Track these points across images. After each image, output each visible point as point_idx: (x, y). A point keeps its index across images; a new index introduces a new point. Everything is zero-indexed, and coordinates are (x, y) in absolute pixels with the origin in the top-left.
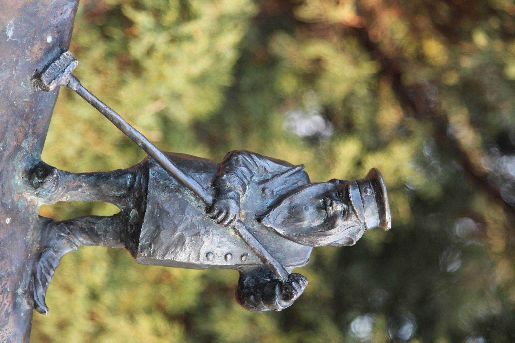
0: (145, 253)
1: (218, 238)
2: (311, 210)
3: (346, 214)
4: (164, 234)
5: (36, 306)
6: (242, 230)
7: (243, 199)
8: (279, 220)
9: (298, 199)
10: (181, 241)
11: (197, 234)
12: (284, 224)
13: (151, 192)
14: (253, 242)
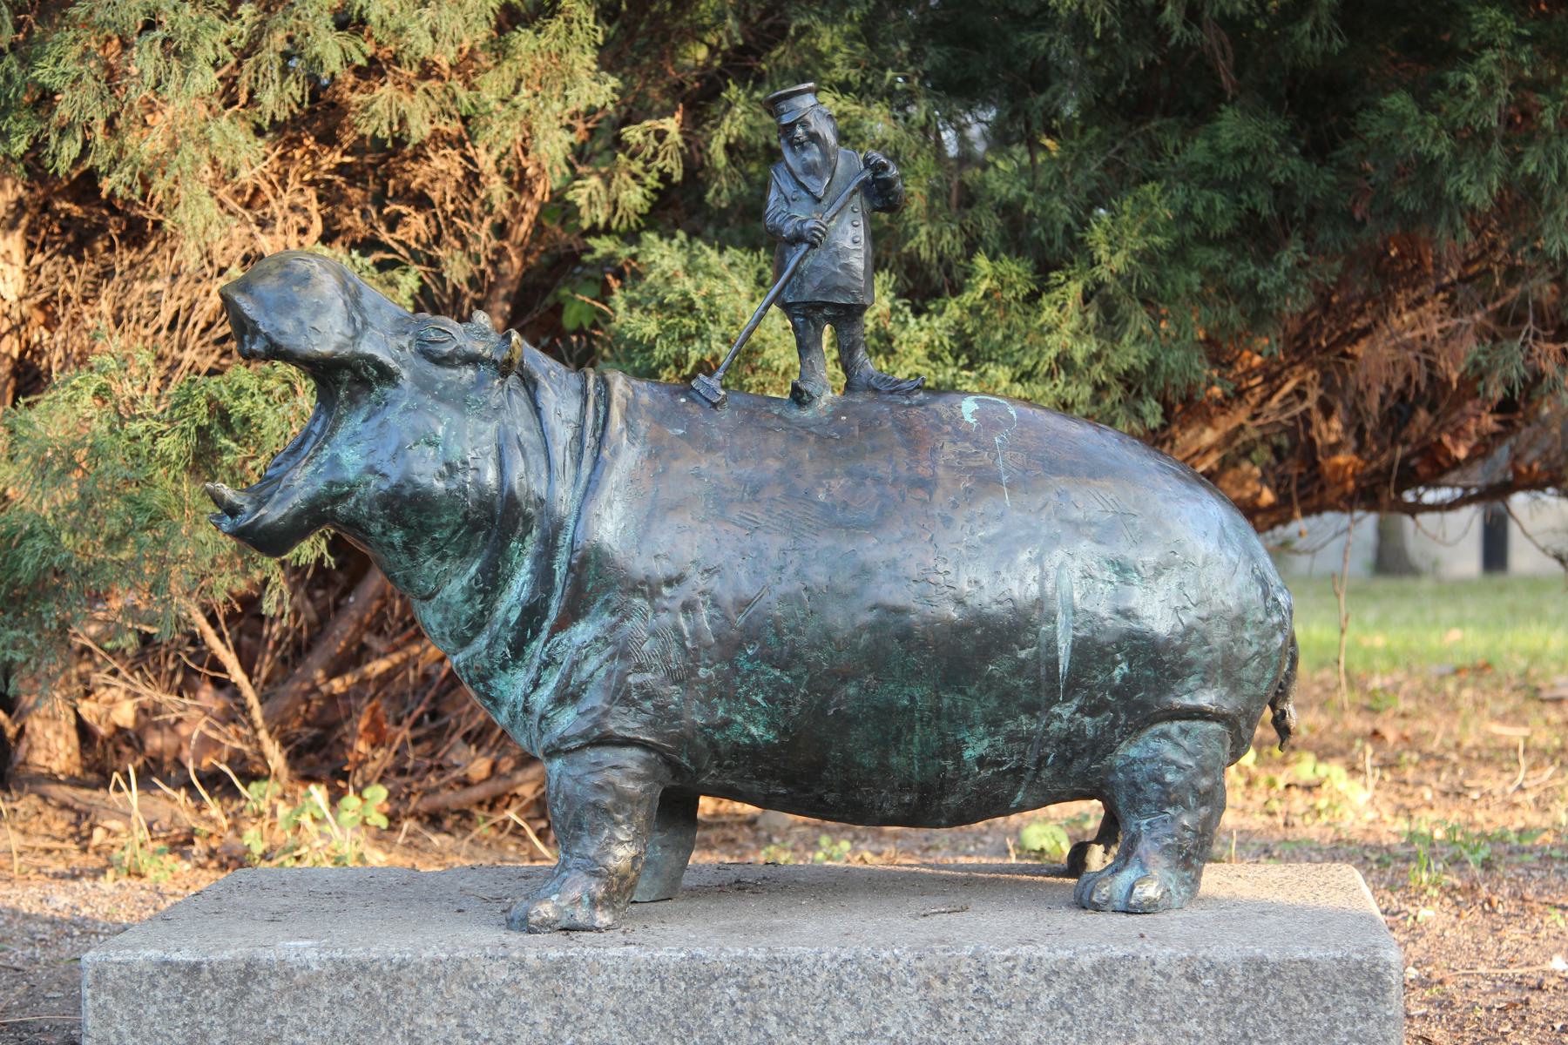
0: (860, 297)
1: (839, 235)
2: (805, 155)
3: (805, 124)
4: (841, 283)
5: (918, 387)
6: (829, 214)
7: (803, 217)
8: (817, 183)
9: (797, 168)
10: (846, 267)
11: (837, 253)
12: (820, 178)
13: (806, 298)
14: (838, 204)
